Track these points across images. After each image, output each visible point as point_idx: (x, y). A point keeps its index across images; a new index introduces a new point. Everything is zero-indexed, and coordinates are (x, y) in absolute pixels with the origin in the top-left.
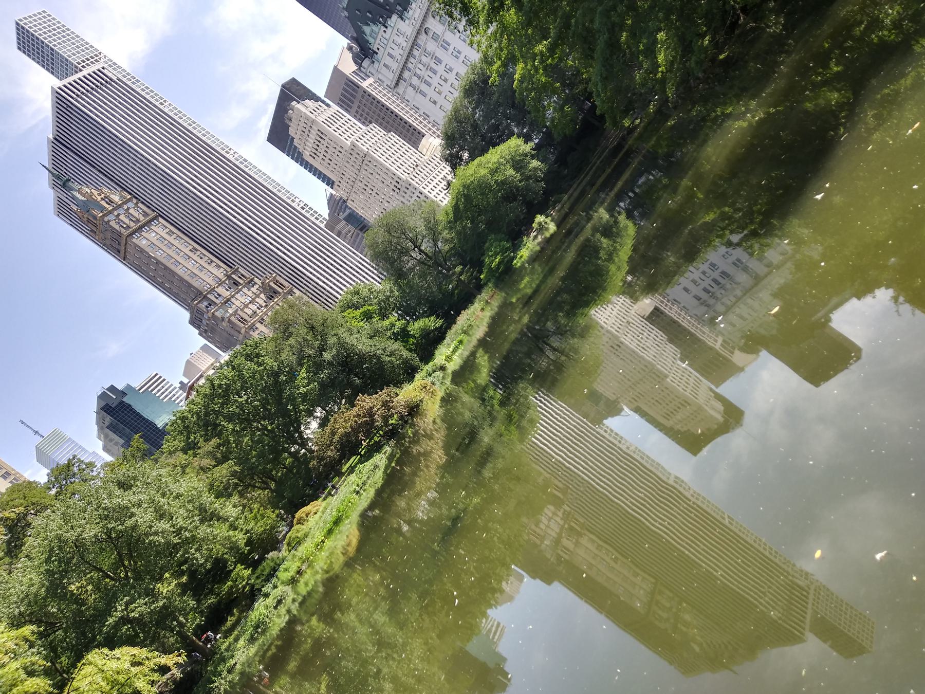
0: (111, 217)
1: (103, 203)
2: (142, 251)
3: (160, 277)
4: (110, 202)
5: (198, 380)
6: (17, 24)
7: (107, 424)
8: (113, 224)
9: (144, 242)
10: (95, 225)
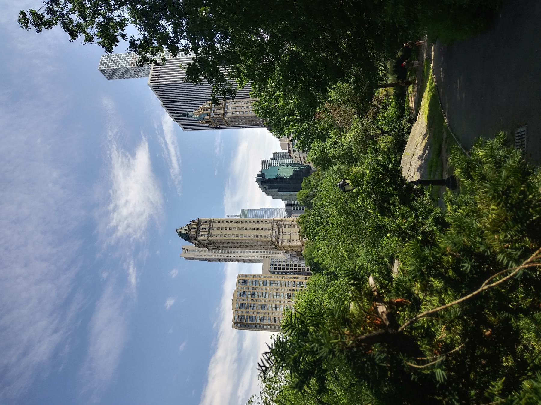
0: (212, 115)
1: (205, 112)
2: (232, 118)
3: (245, 122)
4: (207, 109)
5: (289, 147)
6: (100, 70)
8: (215, 116)
9: (230, 114)
10: (210, 122)
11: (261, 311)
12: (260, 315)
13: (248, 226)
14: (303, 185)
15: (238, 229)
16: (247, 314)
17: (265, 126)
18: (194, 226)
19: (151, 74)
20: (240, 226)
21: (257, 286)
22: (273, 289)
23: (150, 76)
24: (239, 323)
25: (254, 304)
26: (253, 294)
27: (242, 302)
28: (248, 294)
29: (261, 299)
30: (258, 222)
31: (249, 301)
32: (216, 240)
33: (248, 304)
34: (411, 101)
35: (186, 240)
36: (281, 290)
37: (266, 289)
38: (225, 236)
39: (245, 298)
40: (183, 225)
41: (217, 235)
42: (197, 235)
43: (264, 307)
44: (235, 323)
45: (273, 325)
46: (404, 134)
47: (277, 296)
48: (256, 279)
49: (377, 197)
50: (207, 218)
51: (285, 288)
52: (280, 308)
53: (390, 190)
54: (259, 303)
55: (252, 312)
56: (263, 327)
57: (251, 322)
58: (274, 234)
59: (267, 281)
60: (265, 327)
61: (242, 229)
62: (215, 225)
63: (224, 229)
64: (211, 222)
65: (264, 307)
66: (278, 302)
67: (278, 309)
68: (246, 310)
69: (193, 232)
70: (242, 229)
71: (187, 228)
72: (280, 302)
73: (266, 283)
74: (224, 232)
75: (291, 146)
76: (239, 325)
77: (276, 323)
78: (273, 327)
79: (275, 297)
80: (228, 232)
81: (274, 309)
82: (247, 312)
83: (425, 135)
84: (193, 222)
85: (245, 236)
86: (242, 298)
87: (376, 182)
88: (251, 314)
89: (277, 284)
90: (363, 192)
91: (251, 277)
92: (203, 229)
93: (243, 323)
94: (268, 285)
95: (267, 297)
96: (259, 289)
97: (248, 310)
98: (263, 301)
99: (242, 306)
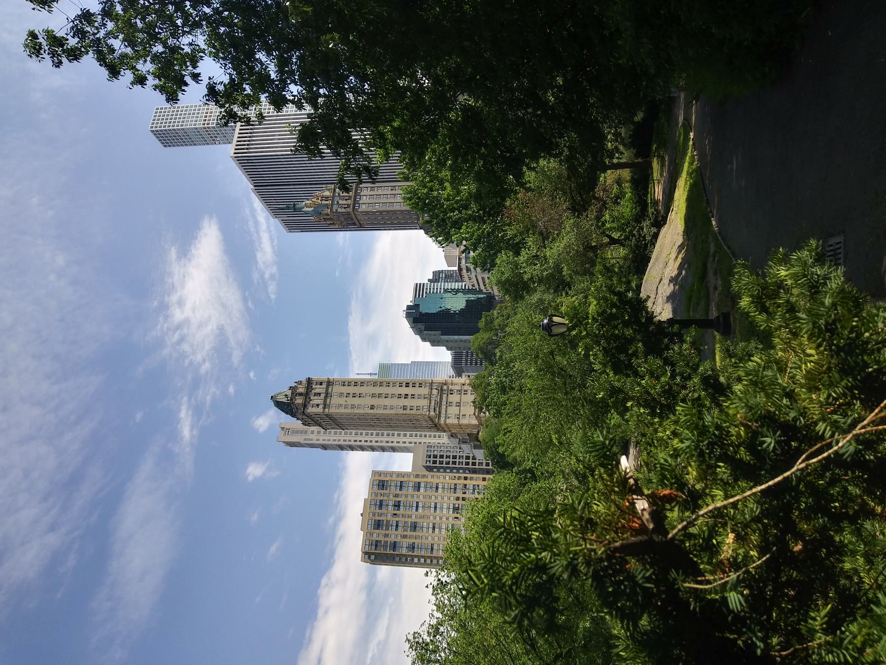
0: (335, 207)
1: (324, 202)
2: (367, 213)
3: (388, 220)
4: (327, 198)
5: (460, 263)
6: (152, 131)
7: (423, 328)
8: (340, 210)
9: (364, 206)
11: (409, 533)
12: (408, 540)
13: (390, 390)
14: (481, 324)
15: (373, 396)
16: (386, 539)
17: (421, 228)
18: (301, 390)
19: (235, 139)
20: (378, 390)
21: (403, 492)
22: (430, 497)
23: (235, 142)
24: (373, 554)
25: (397, 522)
26: (397, 505)
27: (378, 518)
28: (387, 505)
29: (410, 513)
30: (407, 385)
31: (389, 517)
32: (337, 414)
33: (388, 522)
34: (658, 192)
35: (287, 413)
36: (442, 498)
37: (418, 497)
38: (353, 406)
39: (384, 511)
40: (282, 390)
41: (338, 405)
42: (305, 406)
43: (414, 527)
44: (365, 553)
45: (429, 557)
46: (646, 245)
47: (435, 508)
48: (402, 479)
49: (609, 343)
50: (324, 377)
51: (449, 495)
52: (440, 529)
53: (629, 332)
54: (407, 520)
55: (394, 536)
56: (413, 560)
57: (392, 552)
58: (433, 404)
59: (419, 483)
60: (416, 560)
61: (380, 396)
62: (336, 389)
63: (351, 395)
64: (329, 383)
65: (414, 527)
66: (438, 518)
67: (437, 530)
68: (384, 532)
69: (299, 400)
70: (380, 396)
71: (289, 393)
72: (441, 518)
73: (418, 487)
74: (351, 401)
75: (463, 261)
76: (373, 557)
77: (435, 554)
78: (428, 561)
79: (433, 509)
80: (357, 401)
81: (431, 530)
82: (386, 535)
83: (681, 247)
84: (300, 383)
85: (385, 407)
86: (378, 511)
87: (606, 319)
88: (392, 539)
89: (437, 488)
90: (588, 335)
91: (394, 476)
92: (315, 394)
93: (379, 553)
94: (422, 490)
95: (420, 509)
96: (406, 496)
97: (387, 532)
98: (413, 517)
99: (378, 525)
